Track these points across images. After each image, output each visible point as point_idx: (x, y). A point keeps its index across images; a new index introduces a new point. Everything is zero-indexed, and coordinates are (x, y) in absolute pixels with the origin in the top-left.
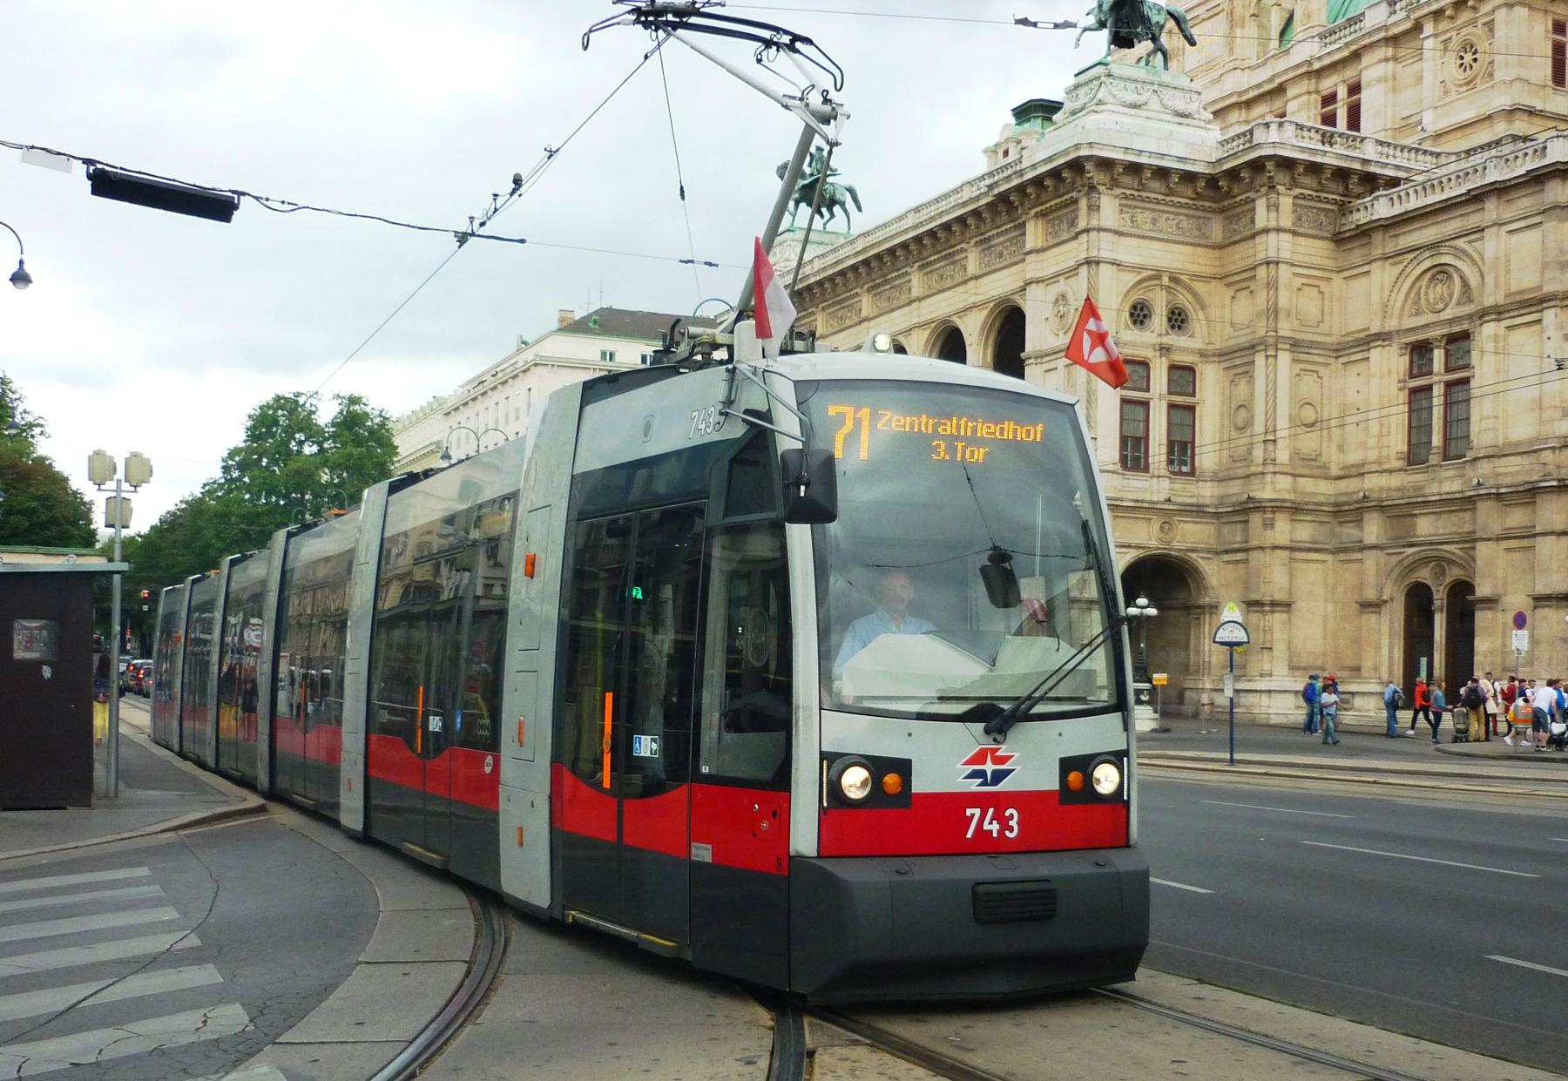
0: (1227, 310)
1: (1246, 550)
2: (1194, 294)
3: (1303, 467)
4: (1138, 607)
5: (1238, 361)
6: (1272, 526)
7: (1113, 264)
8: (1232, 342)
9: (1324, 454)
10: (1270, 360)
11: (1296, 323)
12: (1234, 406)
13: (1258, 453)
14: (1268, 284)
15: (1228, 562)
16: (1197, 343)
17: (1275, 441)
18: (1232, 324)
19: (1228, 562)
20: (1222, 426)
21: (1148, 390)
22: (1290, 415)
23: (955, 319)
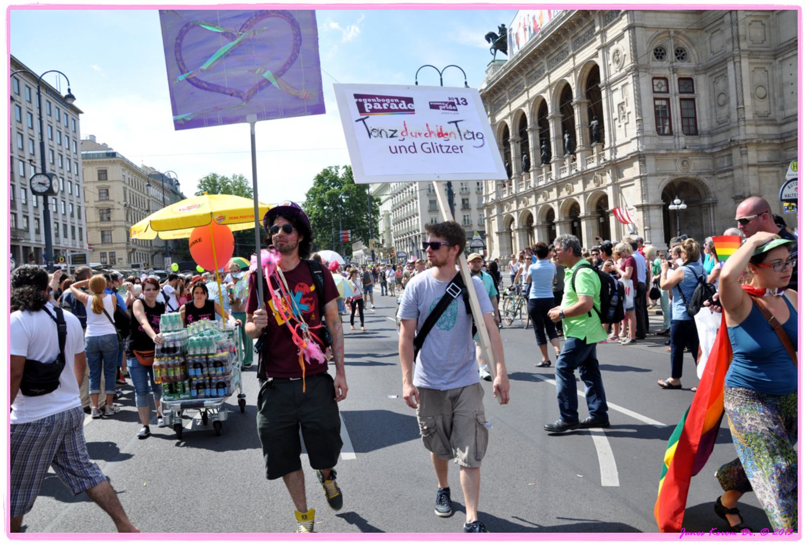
0: (708, 45)
1: (732, 170)
2: (689, 39)
3: (760, 120)
4: (674, 204)
5: (717, 70)
6: (747, 154)
7: (642, 27)
8: (712, 61)
9: (772, 112)
10: (737, 64)
11: (750, 43)
12: (717, 94)
13: (734, 117)
14: (732, 23)
15: (721, 178)
16: (693, 65)
17: (744, 108)
18: (711, 52)
19: (721, 178)
20: (711, 106)
21: (667, 92)
22: (751, 94)
23: (566, 78)
